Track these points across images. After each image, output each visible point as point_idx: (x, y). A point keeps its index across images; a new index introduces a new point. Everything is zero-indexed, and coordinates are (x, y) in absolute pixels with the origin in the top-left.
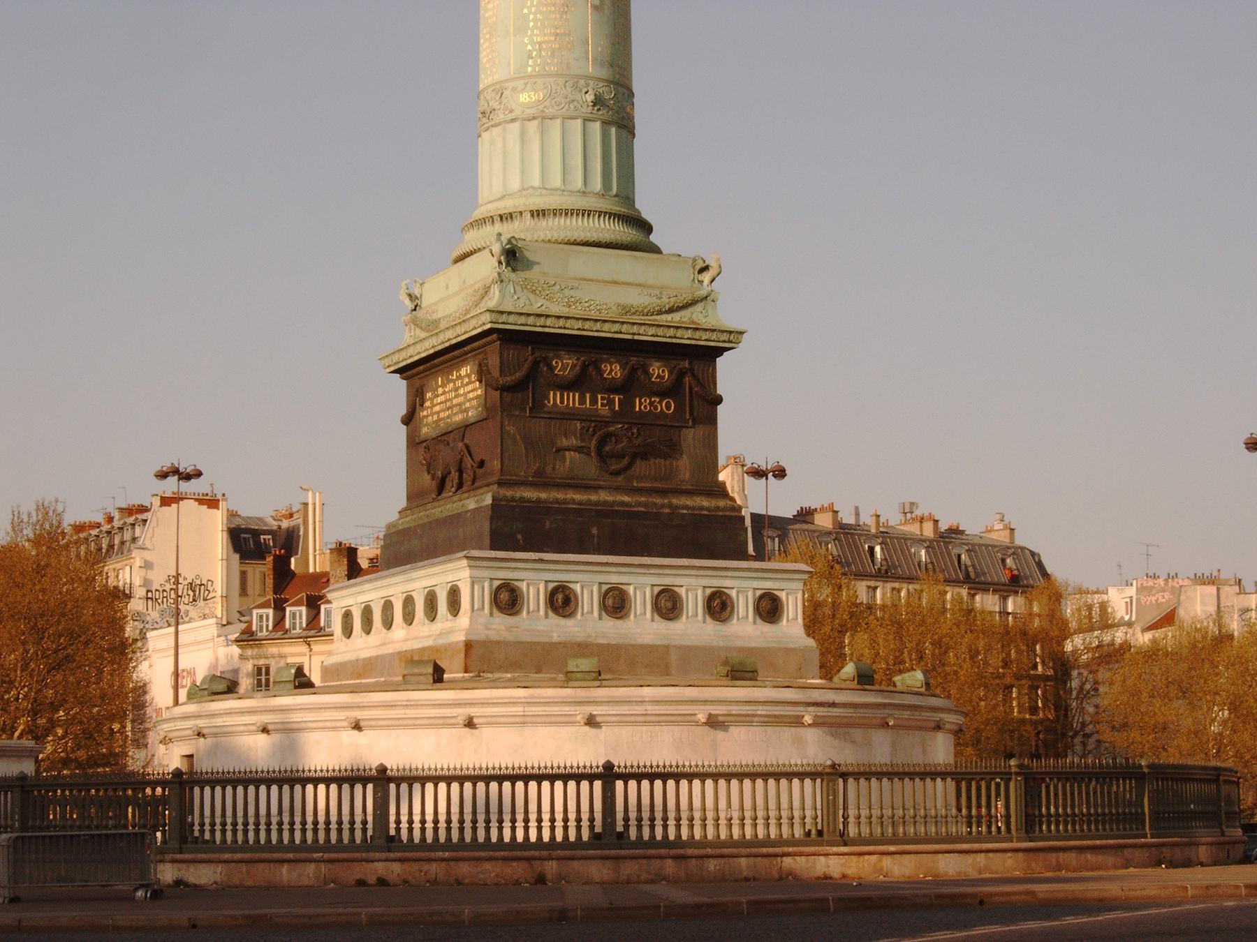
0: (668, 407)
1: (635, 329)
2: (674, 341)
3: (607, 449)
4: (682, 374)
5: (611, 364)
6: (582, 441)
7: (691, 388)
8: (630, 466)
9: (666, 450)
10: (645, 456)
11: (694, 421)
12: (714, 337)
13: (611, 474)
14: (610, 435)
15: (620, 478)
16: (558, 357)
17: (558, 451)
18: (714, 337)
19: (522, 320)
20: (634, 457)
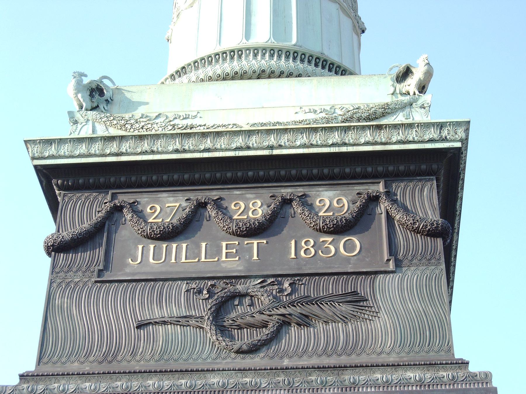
0: (349, 247)
1: (272, 140)
2: (344, 149)
3: (233, 315)
4: (374, 199)
5: (246, 201)
6: (188, 306)
7: (390, 219)
8: (275, 336)
9: (345, 308)
10: (305, 321)
11: (398, 264)
12: (412, 135)
13: (239, 352)
14: (242, 296)
15: (256, 360)
16: (157, 201)
17: (139, 327)
18: (412, 135)
19: (83, 149)
20: (285, 323)
